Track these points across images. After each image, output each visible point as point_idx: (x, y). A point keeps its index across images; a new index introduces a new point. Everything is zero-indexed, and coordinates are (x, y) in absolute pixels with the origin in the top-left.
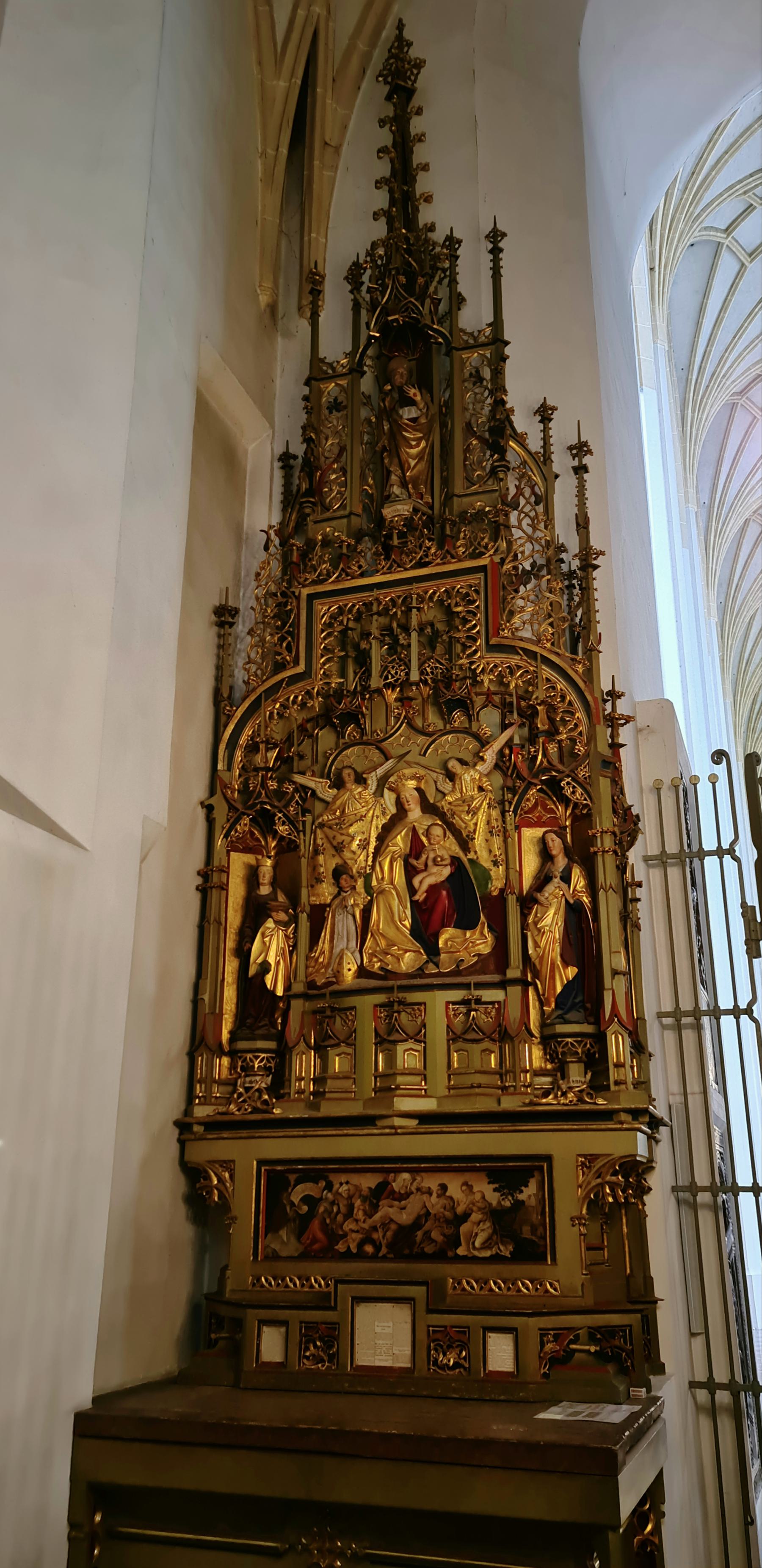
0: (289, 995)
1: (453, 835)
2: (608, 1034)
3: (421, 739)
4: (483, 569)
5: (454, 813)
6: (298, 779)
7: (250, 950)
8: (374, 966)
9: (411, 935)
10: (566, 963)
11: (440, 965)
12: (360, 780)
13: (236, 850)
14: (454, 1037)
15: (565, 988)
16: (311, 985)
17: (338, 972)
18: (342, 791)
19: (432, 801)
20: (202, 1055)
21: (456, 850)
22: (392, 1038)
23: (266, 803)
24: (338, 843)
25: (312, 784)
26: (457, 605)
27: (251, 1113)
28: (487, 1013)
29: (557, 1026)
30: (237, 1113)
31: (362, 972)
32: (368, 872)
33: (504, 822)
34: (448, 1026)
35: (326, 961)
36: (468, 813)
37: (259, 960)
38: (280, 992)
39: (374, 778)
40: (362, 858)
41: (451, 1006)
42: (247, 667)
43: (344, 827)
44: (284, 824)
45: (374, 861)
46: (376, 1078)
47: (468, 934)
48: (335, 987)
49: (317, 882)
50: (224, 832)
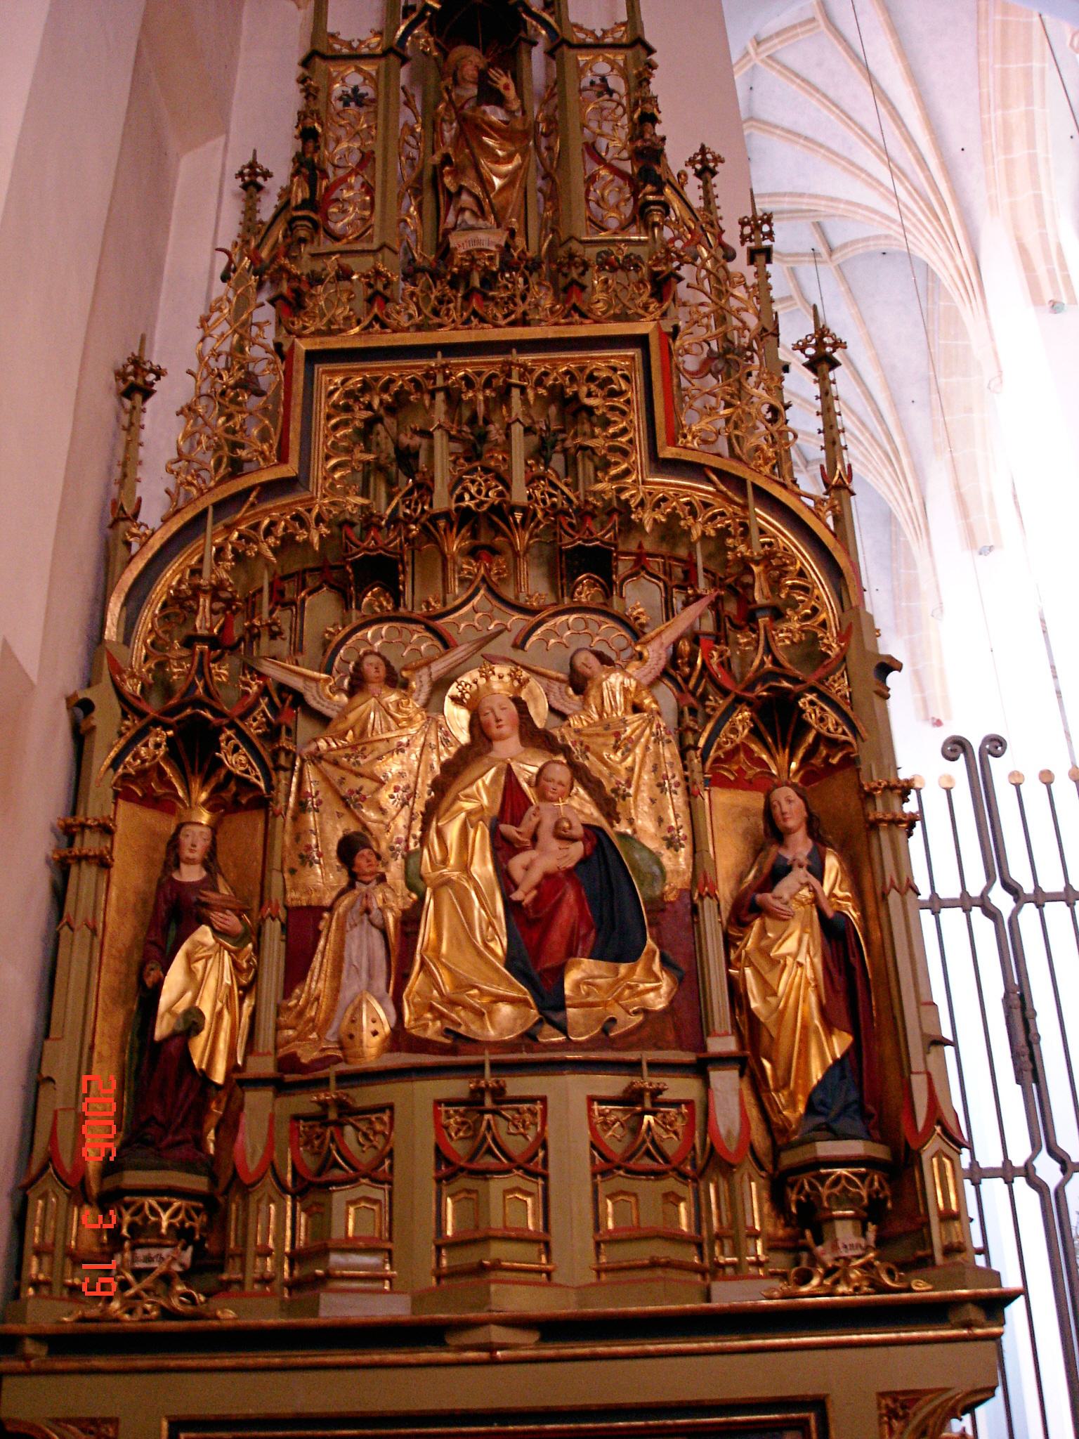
0: (239, 1080)
1: (585, 788)
2: (925, 1157)
3: (516, 621)
4: (641, 341)
5: (587, 748)
6: (268, 668)
7: (159, 985)
8: (425, 1027)
9: (506, 967)
10: (830, 1025)
11: (569, 1029)
12: (394, 680)
13: (128, 796)
14: (605, 1165)
15: (828, 1072)
16: (288, 1063)
17: (351, 1036)
18: (358, 699)
19: (539, 725)
20: (44, 1196)
21: (592, 812)
22: (476, 1165)
23: (204, 706)
24: (351, 792)
25: (297, 683)
26: (589, 395)
27: (157, 1319)
28: (666, 1124)
29: (819, 1144)
30: (127, 1317)
31: (399, 1038)
32: (412, 847)
33: (685, 768)
34: (593, 1146)
35: (322, 1016)
36: (616, 748)
37: (181, 1007)
38: (219, 1077)
39: (425, 679)
40: (401, 822)
41: (596, 1106)
42: (175, 467)
43: (362, 761)
44: (236, 749)
45: (425, 828)
46: (438, 1249)
47: (623, 968)
48: (342, 1067)
49: (303, 864)
50: (112, 754)
